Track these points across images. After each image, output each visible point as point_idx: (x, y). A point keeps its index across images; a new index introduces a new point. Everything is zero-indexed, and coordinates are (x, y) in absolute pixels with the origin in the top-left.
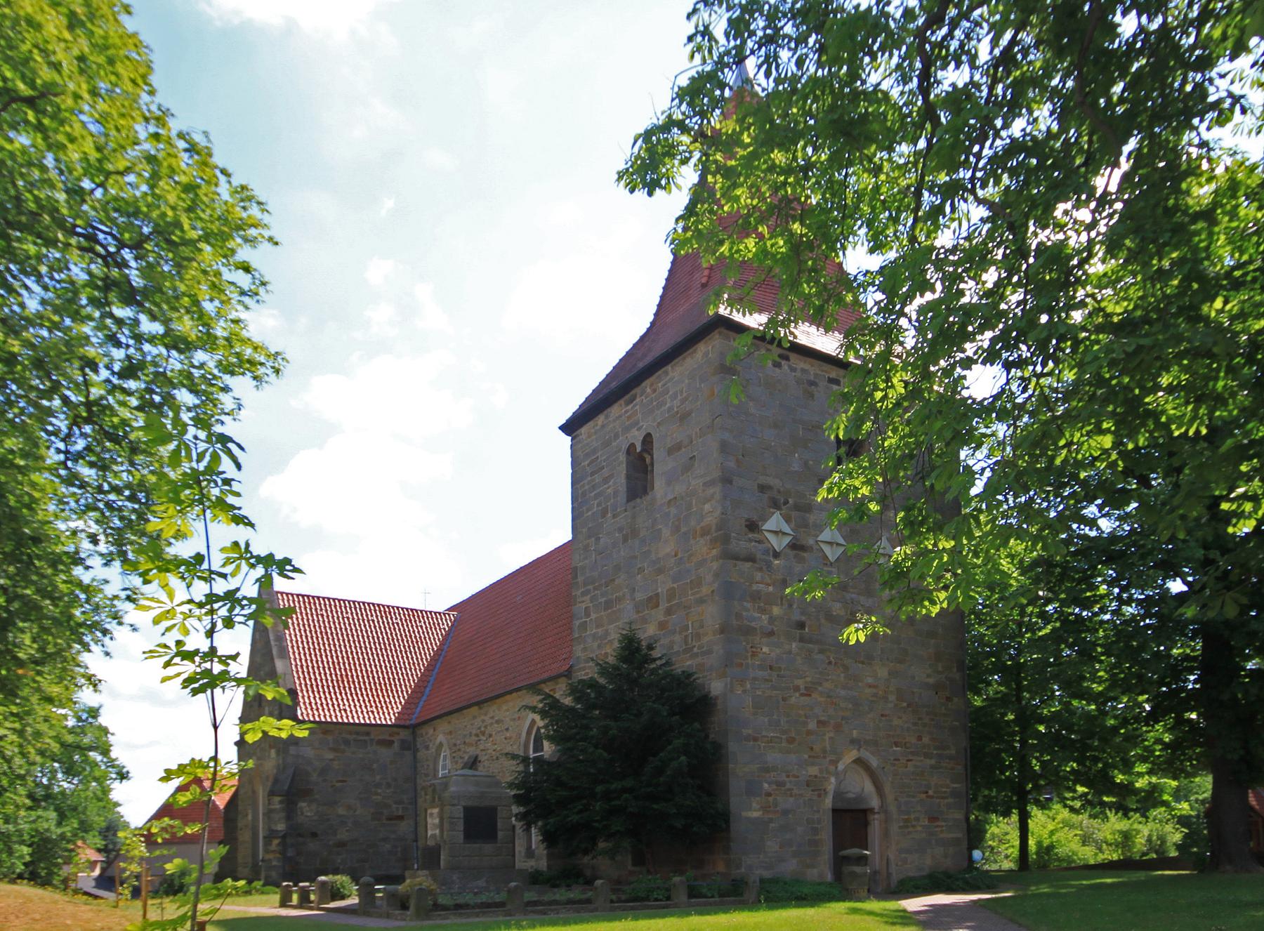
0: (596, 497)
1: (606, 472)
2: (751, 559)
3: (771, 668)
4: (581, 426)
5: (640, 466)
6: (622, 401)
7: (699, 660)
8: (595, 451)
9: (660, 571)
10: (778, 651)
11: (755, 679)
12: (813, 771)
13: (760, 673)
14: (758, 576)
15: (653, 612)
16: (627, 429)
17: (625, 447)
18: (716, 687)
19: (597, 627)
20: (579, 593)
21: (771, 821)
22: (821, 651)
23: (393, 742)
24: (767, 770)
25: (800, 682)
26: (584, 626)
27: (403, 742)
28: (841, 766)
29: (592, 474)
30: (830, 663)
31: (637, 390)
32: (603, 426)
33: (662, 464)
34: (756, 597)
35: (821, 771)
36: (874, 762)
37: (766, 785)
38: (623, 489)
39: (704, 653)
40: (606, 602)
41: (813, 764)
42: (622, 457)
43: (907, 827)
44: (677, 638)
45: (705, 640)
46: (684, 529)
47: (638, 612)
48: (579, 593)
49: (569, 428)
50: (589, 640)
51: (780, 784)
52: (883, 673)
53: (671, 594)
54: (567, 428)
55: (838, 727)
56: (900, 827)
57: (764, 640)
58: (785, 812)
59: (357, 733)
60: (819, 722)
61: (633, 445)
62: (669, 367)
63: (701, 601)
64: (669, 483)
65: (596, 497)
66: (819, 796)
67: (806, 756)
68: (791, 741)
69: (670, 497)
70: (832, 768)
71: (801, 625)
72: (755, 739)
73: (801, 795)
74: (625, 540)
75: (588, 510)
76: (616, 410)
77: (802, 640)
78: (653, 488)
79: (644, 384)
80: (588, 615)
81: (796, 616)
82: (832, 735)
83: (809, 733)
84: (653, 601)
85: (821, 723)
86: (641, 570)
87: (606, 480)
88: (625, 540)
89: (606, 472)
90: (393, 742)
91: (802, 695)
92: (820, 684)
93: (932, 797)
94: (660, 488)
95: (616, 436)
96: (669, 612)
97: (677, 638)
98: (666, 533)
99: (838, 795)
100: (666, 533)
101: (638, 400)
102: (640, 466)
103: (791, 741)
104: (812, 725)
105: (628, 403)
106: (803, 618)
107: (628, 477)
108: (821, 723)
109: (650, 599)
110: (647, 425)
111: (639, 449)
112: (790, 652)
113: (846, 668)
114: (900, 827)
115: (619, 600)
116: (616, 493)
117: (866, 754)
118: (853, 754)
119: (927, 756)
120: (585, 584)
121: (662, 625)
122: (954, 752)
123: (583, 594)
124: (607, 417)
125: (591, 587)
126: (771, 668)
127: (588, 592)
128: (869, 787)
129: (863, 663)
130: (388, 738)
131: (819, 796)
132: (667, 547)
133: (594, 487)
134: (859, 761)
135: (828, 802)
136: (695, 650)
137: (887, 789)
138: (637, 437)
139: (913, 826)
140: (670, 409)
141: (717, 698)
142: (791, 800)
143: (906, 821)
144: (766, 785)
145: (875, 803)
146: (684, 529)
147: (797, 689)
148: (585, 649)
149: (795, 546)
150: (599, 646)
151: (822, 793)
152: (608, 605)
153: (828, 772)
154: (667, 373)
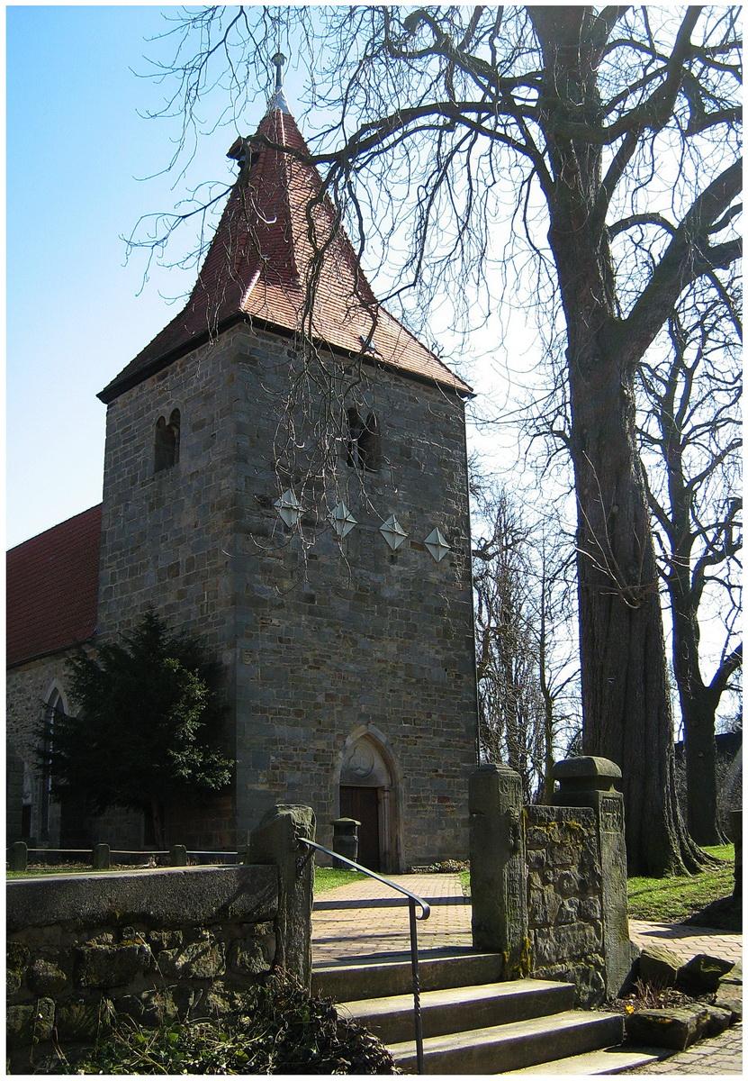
0: (127, 464)
1: (137, 441)
2: (263, 533)
3: (281, 640)
5: (168, 437)
7: (213, 629)
8: (127, 421)
9: (181, 541)
10: (287, 623)
11: (264, 650)
12: (321, 745)
13: (270, 645)
14: (269, 549)
16: (158, 403)
17: (155, 419)
18: (227, 657)
19: (122, 593)
21: (278, 795)
22: (330, 625)
24: (275, 742)
25: (309, 655)
28: (349, 741)
29: (125, 442)
30: (339, 637)
33: (188, 439)
34: (266, 569)
36: (383, 738)
37: (273, 758)
38: (151, 459)
39: (217, 624)
41: (320, 738)
42: (153, 429)
43: (416, 806)
44: (194, 607)
45: (219, 609)
46: (203, 502)
47: (160, 580)
49: (105, 396)
51: (287, 757)
52: (392, 648)
53: (191, 563)
54: (105, 396)
55: (346, 702)
56: (409, 806)
57: (274, 612)
60: (327, 695)
63: (216, 572)
64: (192, 457)
65: (127, 464)
66: (327, 771)
67: (314, 730)
68: (299, 713)
71: (311, 599)
72: (264, 711)
73: (308, 769)
74: (152, 508)
75: (119, 476)
76: (148, 384)
77: (311, 612)
78: (178, 461)
80: (113, 581)
81: (307, 590)
82: (339, 709)
83: (317, 706)
84: (174, 570)
85: (329, 696)
86: (164, 539)
87: (137, 449)
88: (152, 508)
89: (137, 441)
91: (310, 667)
92: (329, 657)
93: (441, 776)
94: (185, 463)
95: (148, 408)
97: (194, 607)
98: (188, 503)
99: (347, 772)
100: (188, 503)
102: (168, 437)
103: (299, 713)
104: (321, 699)
105: (160, 379)
106: (313, 592)
107: (157, 448)
108: (329, 696)
109: (171, 567)
110: (176, 401)
111: (167, 423)
112: (299, 625)
113: (355, 642)
114: (409, 806)
115: (144, 566)
116: (145, 462)
117: (374, 729)
118: (360, 731)
119: (436, 733)
121: (181, 594)
122: (464, 730)
124: (141, 389)
125: (118, 553)
126: (281, 640)
127: (116, 557)
128: (379, 764)
129: (371, 637)
131: (327, 771)
132: (188, 519)
133: (125, 455)
134: (368, 737)
135: (336, 777)
136: (210, 620)
137: (397, 766)
138: (166, 410)
139: (424, 806)
141: (227, 668)
142: (299, 773)
143: (415, 800)
144: (273, 758)
145: (384, 781)
146: (203, 502)
147: (305, 661)
148: (108, 616)
149: (307, 522)
150: (123, 614)
152: (133, 571)
153: (335, 747)
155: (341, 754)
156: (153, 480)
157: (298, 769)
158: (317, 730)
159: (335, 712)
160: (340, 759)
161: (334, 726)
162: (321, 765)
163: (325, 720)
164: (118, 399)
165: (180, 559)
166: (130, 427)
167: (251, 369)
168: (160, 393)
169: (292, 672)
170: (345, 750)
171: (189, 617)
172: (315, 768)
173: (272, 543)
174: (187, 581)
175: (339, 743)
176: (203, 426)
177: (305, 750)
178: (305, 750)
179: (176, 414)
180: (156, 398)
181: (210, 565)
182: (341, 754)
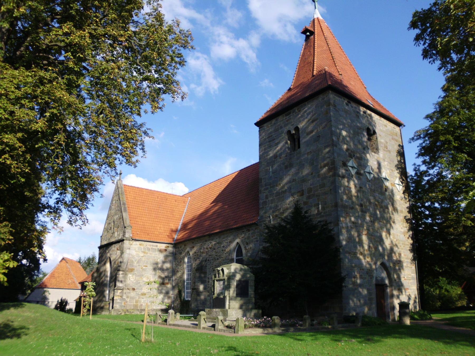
4: (264, 123)
6: (284, 115)
20: (263, 189)
26: (265, 203)
29: (269, 142)
31: (292, 111)
32: (275, 124)
48: (263, 189)
54: (257, 124)
59: (153, 246)
61: (289, 132)
62: (306, 103)
66: (371, 278)
69: (308, 151)
76: (280, 118)
78: (299, 147)
79: (294, 109)
94: (303, 148)
95: (281, 127)
96: (309, 197)
101: (291, 114)
102: (295, 138)
105: (286, 115)
120: (266, 186)
123: (264, 190)
124: (277, 120)
125: (269, 187)
127: (267, 189)
131: (371, 278)
135: (374, 281)
136: (322, 214)
151: (371, 277)
165: (304, 189)
166: (272, 136)
168: (287, 121)
180: (285, 125)
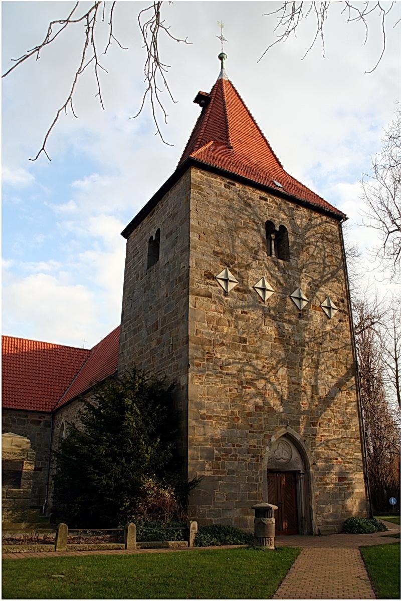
12: (253, 442)
15: (155, 333)
23: (40, 422)
27: (46, 422)
28: (273, 439)
33: (164, 244)
35: (258, 443)
38: (146, 262)
39: (178, 358)
40: (134, 330)
41: (253, 437)
42: (147, 244)
50: (126, 354)
58: (231, 473)
64: (166, 254)
66: (257, 460)
67: (247, 431)
70: (267, 440)
73: (243, 460)
76: (145, 221)
84: (155, 326)
90: (40, 422)
97: (166, 348)
99: (272, 460)
100: (163, 283)
101: (155, 213)
107: (149, 255)
118: (283, 431)
121: (159, 342)
128: (295, 455)
130: (38, 419)
131: (257, 460)
135: (265, 466)
140: (169, 213)
142: (236, 463)
145: (300, 467)
146: (171, 280)
154: (168, 195)
155: (267, 449)
156: (146, 274)
157: (236, 460)
158: (250, 432)
159: (262, 418)
160: (267, 452)
161: (262, 429)
162: (252, 457)
163: (255, 425)
164: (132, 234)
167: (199, 193)
168: (151, 223)
169: (230, 391)
170: (270, 445)
171: (162, 355)
172: (249, 459)
173: (215, 302)
174: (162, 333)
175: (267, 440)
176: (171, 234)
177: (241, 446)
178: (241, 446)
179: (158, 231)
181: (174, 319)
182: (267, 449)
